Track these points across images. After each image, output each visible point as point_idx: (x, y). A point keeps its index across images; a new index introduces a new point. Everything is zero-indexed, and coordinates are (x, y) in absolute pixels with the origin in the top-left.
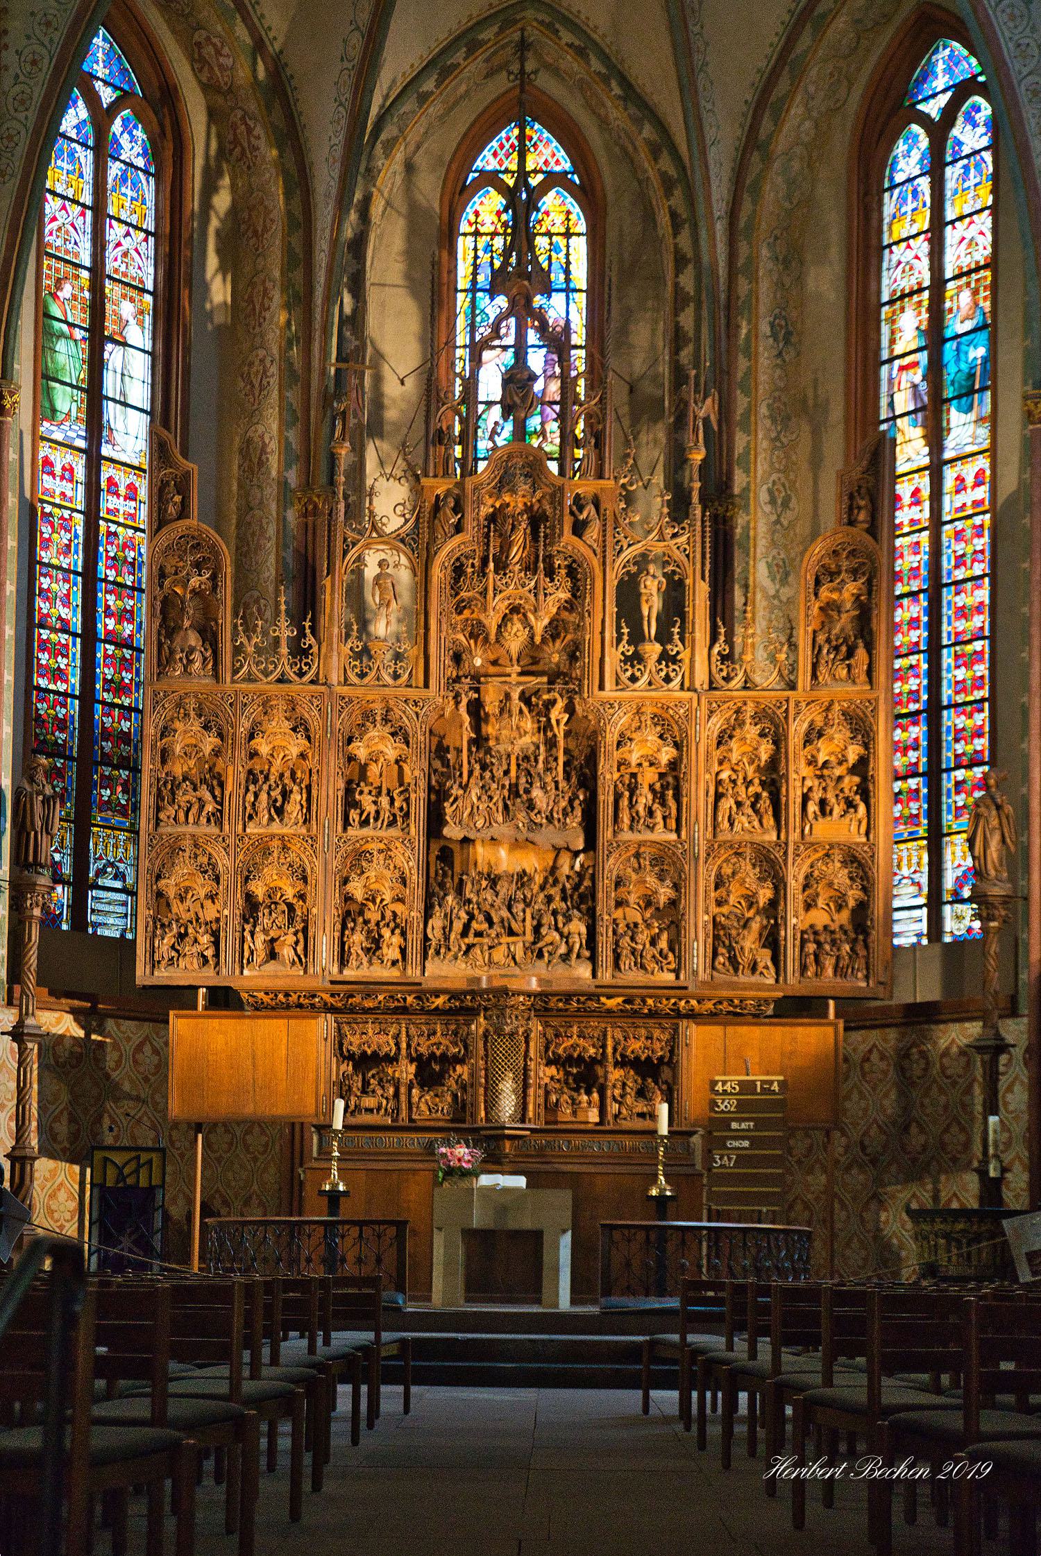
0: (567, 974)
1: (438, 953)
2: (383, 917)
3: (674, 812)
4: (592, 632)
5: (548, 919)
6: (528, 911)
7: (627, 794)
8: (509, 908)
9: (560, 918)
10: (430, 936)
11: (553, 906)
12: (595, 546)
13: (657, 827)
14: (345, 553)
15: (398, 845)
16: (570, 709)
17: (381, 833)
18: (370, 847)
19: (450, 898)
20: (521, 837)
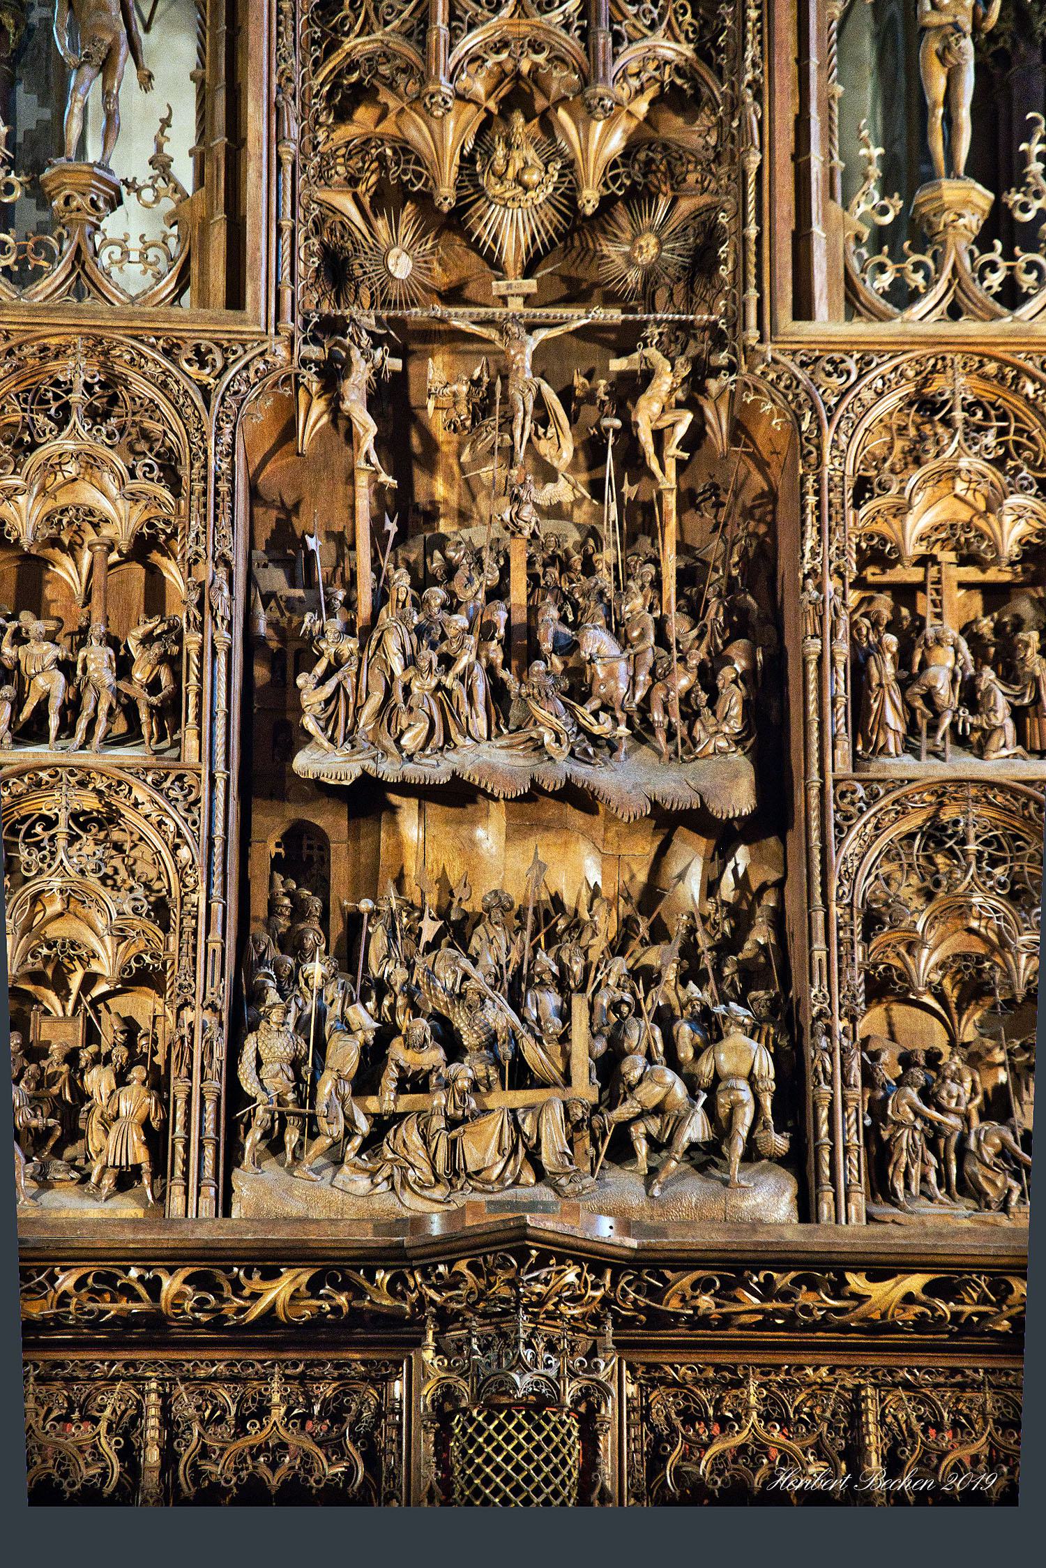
0: (716, 1210)
1: (274, 1144)
2: (92, 1035)
4: (768, 148)
5: (642, 1033)
6: (579, 1006)
7: (891, 640)
8: (516, 1003)
10: (249, 1085)
11: (657, 998)
13: (997, 740)
15: (140, 794)
18: (48, 804)
19: (316, 969)
20: (553, 778)
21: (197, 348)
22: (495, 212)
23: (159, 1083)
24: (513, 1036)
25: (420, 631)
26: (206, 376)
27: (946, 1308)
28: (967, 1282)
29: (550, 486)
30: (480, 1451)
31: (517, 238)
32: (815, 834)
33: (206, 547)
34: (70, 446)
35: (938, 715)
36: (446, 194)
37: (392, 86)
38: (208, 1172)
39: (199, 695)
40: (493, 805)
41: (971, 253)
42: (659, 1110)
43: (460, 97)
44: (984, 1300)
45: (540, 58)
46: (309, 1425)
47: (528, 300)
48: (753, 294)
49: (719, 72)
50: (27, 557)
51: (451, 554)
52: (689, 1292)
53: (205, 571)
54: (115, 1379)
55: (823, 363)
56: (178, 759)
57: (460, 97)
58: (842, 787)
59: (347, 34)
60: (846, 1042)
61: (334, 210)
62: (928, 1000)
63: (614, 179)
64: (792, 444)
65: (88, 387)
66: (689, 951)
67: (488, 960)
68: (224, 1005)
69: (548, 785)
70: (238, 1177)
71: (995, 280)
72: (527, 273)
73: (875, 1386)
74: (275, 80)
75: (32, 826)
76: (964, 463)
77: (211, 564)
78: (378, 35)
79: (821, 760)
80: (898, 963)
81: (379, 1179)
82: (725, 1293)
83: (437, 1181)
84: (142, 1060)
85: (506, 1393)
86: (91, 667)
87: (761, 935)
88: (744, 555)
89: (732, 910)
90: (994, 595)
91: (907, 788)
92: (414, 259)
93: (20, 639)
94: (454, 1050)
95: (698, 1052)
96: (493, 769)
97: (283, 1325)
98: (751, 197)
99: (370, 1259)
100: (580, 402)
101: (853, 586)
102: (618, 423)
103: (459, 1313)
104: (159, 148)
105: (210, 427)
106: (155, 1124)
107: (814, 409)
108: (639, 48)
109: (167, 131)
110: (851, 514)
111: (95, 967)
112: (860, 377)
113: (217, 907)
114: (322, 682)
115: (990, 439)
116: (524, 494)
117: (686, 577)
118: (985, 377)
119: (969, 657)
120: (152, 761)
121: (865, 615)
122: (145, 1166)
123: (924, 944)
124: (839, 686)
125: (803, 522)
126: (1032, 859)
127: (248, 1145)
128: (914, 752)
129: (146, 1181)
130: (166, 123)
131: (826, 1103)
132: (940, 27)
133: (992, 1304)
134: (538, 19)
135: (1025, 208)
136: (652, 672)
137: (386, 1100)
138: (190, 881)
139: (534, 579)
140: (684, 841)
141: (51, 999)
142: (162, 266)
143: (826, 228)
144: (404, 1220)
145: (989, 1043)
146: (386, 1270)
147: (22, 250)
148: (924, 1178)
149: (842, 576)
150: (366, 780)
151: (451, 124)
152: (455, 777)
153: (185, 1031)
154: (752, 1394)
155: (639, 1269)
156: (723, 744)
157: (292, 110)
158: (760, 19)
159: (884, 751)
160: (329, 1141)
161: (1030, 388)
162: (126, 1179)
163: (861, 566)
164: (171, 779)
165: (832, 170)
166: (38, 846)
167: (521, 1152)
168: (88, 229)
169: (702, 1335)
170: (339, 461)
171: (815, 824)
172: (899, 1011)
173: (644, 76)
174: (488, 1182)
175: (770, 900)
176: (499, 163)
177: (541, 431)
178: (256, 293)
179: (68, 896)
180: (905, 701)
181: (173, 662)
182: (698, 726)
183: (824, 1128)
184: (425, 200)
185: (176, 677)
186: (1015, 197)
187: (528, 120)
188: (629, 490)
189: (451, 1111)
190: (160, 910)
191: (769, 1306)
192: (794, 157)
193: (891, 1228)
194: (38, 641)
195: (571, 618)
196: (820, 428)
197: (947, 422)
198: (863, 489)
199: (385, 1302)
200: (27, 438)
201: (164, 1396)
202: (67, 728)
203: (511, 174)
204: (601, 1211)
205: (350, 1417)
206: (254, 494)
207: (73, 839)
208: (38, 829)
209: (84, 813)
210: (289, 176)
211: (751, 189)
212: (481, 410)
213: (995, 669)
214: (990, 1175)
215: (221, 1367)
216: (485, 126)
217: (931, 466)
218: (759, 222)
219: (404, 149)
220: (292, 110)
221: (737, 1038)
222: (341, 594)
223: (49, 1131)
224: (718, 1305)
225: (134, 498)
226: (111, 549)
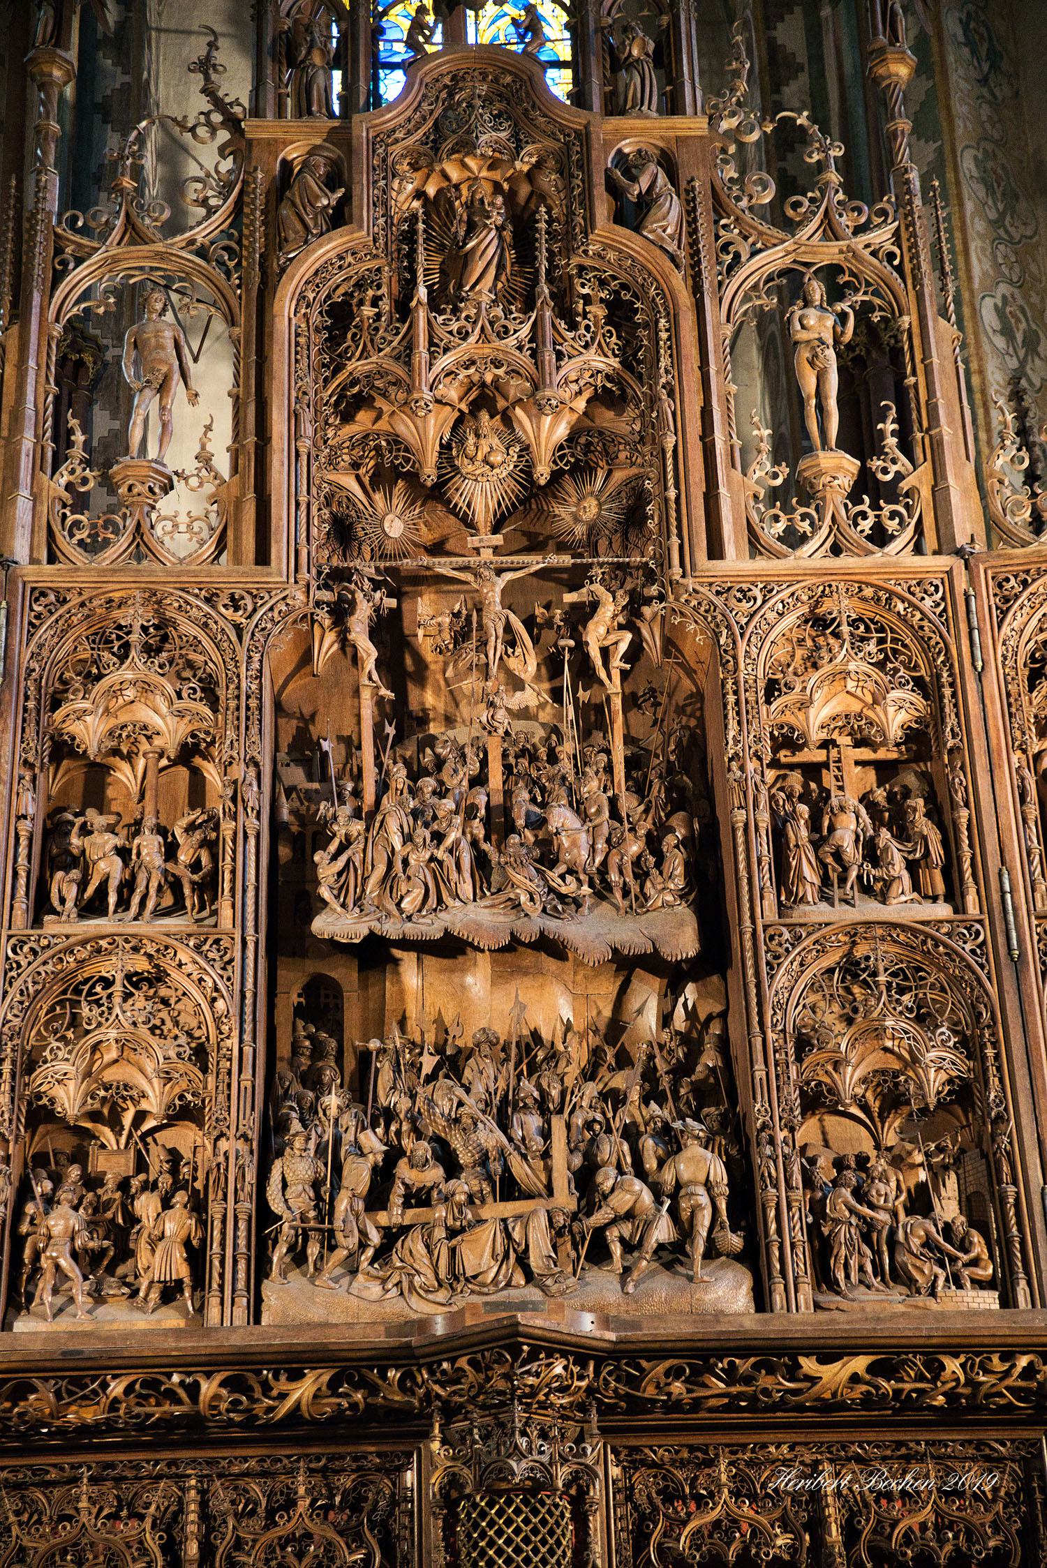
0: (682, 1303)
1: (298, 1258)
2: (141, 1165)
3: (936, 850)
4: (683, 432)
5: (612, 1148)
6: (558, 1124)
8: (504, 1126)
9: (649, 1145)
10: (276, 1206)
11: (624, 1116)
12: (672, 247)
13: (896, 888)
14: (58, 278)
16: (631, 618)
17: (141, 928)
19: (333, 1101)
20: (528, 931)
21: (232, 597)
22: (469, 483)
23: (198, 1206)
24: (502, 1154)
25: (415, 814)
26: (239, 617)
27: (887, 1386)
28: (905, 1362)
29: (518, 694)
30: (483, 1535)
31: (487, 505)
32: (750, 972)
33: (238, 752)
34: (129, 675)
35: (846, 869)
36: (429, 473)
37: (385, 395)
38: (241, 1285)
39: (233, 872)
40: (479, 955)
41: (846, 505)
42: (630, 1215)
43: (438, 401)
44: (920, 1378)
45: (500, 372)
46: (331, 1515)
47: (496, 550)
48: (675, 541)
49: (640, 377)
50: (93, 765)
51: (439, 750)
52: (663, 1380)
53: (238, 771)
54: (159, 1477)
55: (734, 592)
56: (216, 926)
57: (438, 401)
58: (771, 931)
59: (349, 359)
60: (786, 1150)
61: (341, 488)
62: (854, 1110)
63: (562, 458)
64: (713, 655)
65: (144, 629)
66: (649, 1075)
67: (479, 1088)
68: (254, 1135)
69: (525, 938)
70: (268, 1288)
71: (866, 525)
72: (495, 530)
73: (831, 1461)
74: (294, 394)
75: (93, 986)
76: (852, 666)
77: (243, 765)
78: (374, 359)
79: (752, 909)
80: (828, 1080)
81: (389, 1286)
82: (694, 1381)
83: (440, 1285)
84: (185, 1188)
85: (504, 1479)
86: (144, 852)
87: (710, 1059)
88: (679, 744)
89: (684, 1038)
90: (885, 770)
91: (825, 930)
92: (405, 522)
93: (85, 831)
94: (452, 1168)
95: (661, 1164)
96: (479, 926)
97: (307, 1423)
98: (670, 468)
99: (384, 1358)
100: (540, 627)
101: (769, 766)
102: (572, 643)
103: (461, 1406)
104: (203, 447)
105: (242, 656)
106: (195, 1243)
107: (729, 627)
108: (576, 362)
109: (210, 434)
110: (764, 708)
111: (144, 1105)
112: (764, 602)
113: (248, 1050)
114: (335, 857)
115: (872, 647)
116: (497, 701)
117: (632, 763)
118: (864, 599)
119: (868, 821)
120: (194, 928)
121: (781, 789)
122: (187, 1280)
123: (848, 1063)
124: (763, 848)
125: (726, 717)
126: (932, 986)
127: (275, 1259)
128: (829, 900)
129: (187, 1295)
130: (209, 428)
131: (773, 1204)
132: (808, 342)
133: (928, 1381)
134: (497, 343)
135: (885, 471)
136: (608, 841)
137: (395, 1214)
138: (225, 1028)
139: (508, 769)
140: (641, 980)
141: (107, 1134)
142: (205, 534)
143: (729, 490)
144: (414, 1321)
145: (909, 1146)
146: (397, 1368)
147: (94, 526)
148: (861, 1269)
149: (760, 759)
150: (372, 938)
151: (432, 420)
152: (447, 933)
153: (221, 1159)
154: (723, 1472)
155: (618, 1360)
156: (669, 898)
157: (307, 415)
158: (669, 339)
159: (803, 900)
160: (345, 1252)
161: (900, 607)
162: (170, 1293)
163: (775, 750)
164: (209, 942)
165: (732, 447)
166: (98, 1003)
167: (512, 1256)
168: (147, 509)
169: (676, 1418)
170: (347, 679)
171: (749, 963)
172: (830, 1120)
173: (582, 382)
174: (484, 1285)
175: (715, 1029)
176: (471, 449)
177: (510, 650)
178: (279, 551)
179: (122, 1045)
180: (817, 858)
181: (212, 846)
182: (648, 884)
183: (773, 1227)
184: (413, 478)
185: (214, 858)
186: (876, 464)
187: (492, 417)
188: (583, 695)
189: (450, 1222)
190: (200, 1054)
191: (734, 1390)
192: (702, 438)
193: (836, 1314)
194: (100, 832)
195: (539, 799)
196: (734, 642)
197: (836, 635)
198: (772, 689)
199: (397, 1398)
200: (95, 671)
201: (202, 1492)
202: (123, 904)
203: (480, 456)
204: (583, 1308)
205: (367, 1506)
206: (278, 707)
207: (127, 996)
208: (98, 989)
209: (137, 973)
210: (305, 463)
211: (670, 462)
212: (461, 636)
213: (890, 829)
214: (918, 1263)
215: (253, 1463)
216: (459, 422)
217: (826, 669)
218: (677, 486)
219: (395, 441)
220: (307, 415)
221: (694, 1150)
222: (350, 786)
223: (104, 1251)
224: (689, 1391)
225: (180, 714)
226: (161, 756)
